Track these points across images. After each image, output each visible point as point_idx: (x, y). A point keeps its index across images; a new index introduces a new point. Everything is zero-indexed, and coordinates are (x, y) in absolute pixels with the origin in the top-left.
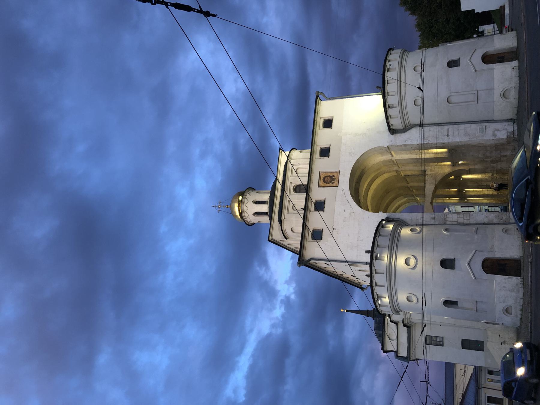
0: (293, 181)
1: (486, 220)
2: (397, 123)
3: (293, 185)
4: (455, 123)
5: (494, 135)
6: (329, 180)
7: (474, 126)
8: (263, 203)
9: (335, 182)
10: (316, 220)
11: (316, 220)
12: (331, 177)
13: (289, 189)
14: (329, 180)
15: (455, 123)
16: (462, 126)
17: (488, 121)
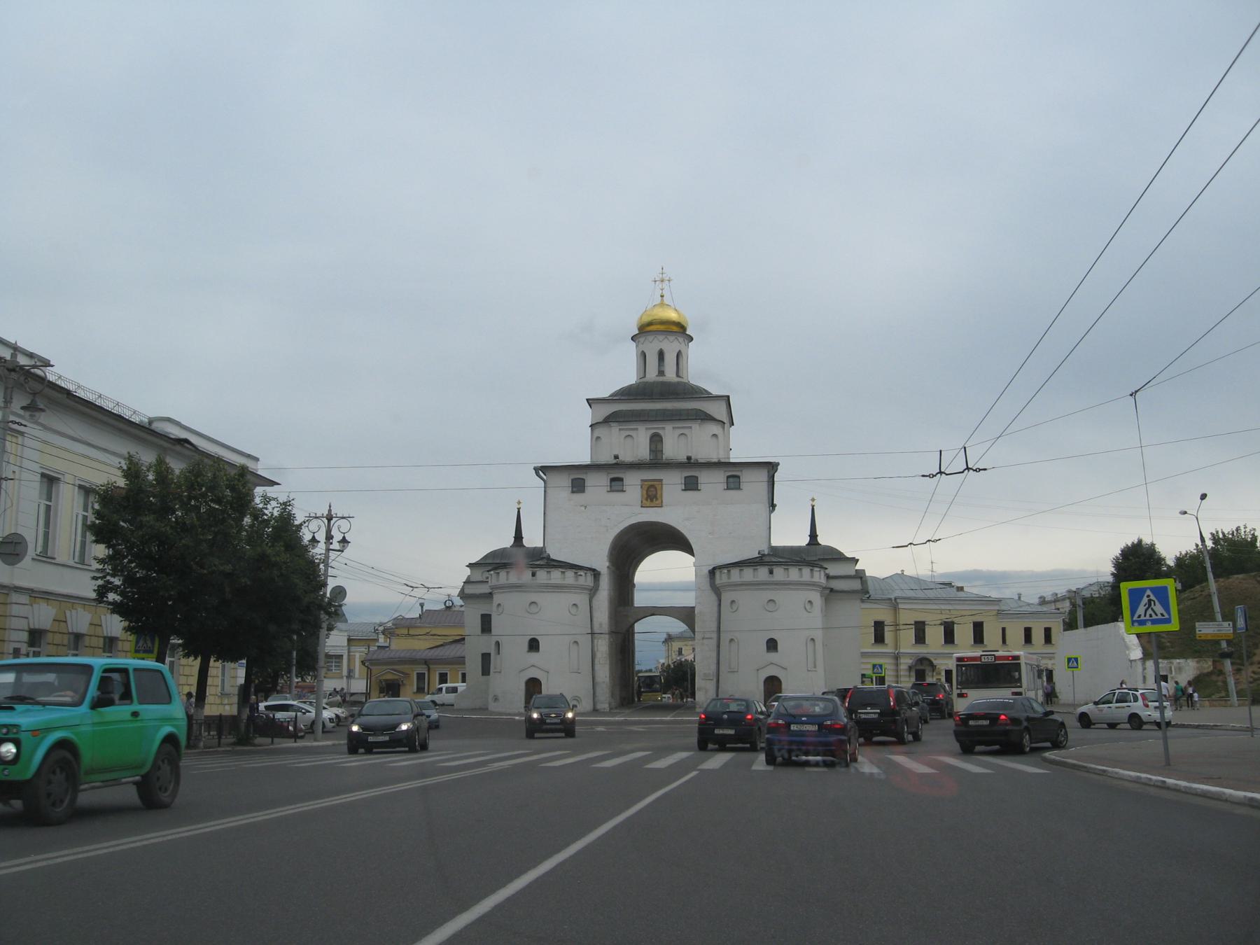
0: (670, 433)
1: (598, 679)
2: (721, 578)
3: (660, 432)
4: (718, 646)
5: (700, 689)
6: (652, 495)
7: (714, 667)
8: (661, 373)
9: (648, 503)
10: (597, 484)
11: (597, 484)
12: (655, 496)
13: (656, 427)
14: (652, 495)
15: (718, 646)
16: (714, 654)
17: (718, 681)
